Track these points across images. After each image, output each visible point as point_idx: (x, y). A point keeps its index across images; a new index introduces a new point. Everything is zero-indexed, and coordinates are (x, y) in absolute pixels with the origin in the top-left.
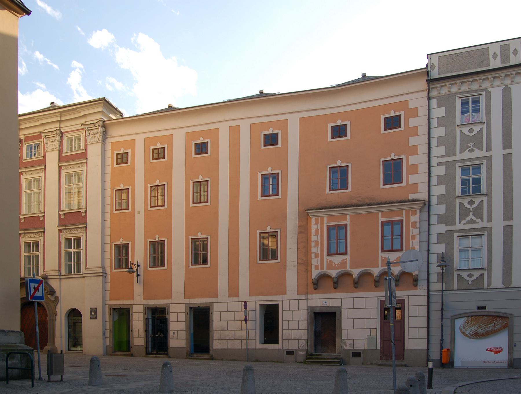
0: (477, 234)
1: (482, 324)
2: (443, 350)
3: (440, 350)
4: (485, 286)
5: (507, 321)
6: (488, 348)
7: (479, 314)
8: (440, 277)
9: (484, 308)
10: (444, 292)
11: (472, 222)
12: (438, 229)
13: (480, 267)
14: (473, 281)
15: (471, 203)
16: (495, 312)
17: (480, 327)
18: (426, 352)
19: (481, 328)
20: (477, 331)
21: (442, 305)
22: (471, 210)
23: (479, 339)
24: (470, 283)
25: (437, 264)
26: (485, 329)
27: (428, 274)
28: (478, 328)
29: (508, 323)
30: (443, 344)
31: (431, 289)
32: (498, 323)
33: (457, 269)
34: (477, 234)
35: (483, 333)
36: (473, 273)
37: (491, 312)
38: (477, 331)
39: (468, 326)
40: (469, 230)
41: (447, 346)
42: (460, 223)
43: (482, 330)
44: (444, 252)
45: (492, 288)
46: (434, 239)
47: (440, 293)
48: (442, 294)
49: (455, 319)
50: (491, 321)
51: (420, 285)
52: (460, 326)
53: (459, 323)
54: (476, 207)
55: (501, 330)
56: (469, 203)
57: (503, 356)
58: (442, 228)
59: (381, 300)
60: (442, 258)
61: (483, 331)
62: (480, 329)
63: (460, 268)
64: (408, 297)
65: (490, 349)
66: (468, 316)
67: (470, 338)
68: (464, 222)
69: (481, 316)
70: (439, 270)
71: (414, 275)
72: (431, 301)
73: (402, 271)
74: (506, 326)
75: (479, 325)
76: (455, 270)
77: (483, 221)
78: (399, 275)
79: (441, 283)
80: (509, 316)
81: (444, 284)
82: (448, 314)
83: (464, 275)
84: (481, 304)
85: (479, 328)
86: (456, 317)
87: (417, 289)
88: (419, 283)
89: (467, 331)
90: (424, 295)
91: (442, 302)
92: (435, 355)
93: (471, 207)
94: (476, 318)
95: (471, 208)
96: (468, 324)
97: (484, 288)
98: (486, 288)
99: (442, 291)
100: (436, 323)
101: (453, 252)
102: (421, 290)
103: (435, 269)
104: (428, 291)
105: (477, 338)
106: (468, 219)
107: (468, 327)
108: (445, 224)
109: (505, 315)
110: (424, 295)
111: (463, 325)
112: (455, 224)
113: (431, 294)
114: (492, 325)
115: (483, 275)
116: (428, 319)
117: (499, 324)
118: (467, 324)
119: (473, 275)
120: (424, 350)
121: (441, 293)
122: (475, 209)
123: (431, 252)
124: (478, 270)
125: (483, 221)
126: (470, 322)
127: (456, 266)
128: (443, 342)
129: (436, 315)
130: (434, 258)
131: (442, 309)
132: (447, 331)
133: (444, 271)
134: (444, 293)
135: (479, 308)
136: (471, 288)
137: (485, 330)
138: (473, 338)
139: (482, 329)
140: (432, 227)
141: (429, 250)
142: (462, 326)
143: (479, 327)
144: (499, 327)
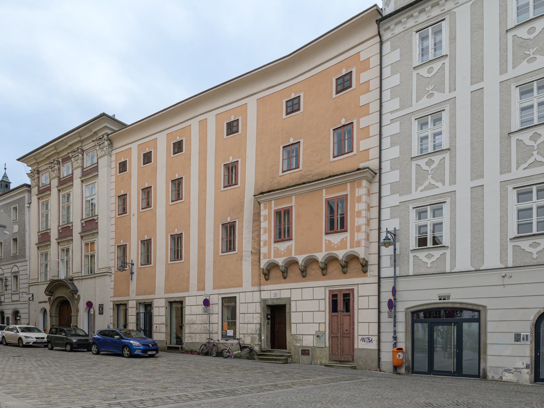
22: (430, 172)
31: (382, 275)
42: (416, 191)
45: (456, 271)
51: (370, 272)
64: (357, 285)
77: (444, 185)
87: (367, 276)
88: (370, 268)
95: (430, 170)
97: (447, 272)
102: (371, 277)
106: (426, 184)
121: (393, 280)
125: (444, 185)
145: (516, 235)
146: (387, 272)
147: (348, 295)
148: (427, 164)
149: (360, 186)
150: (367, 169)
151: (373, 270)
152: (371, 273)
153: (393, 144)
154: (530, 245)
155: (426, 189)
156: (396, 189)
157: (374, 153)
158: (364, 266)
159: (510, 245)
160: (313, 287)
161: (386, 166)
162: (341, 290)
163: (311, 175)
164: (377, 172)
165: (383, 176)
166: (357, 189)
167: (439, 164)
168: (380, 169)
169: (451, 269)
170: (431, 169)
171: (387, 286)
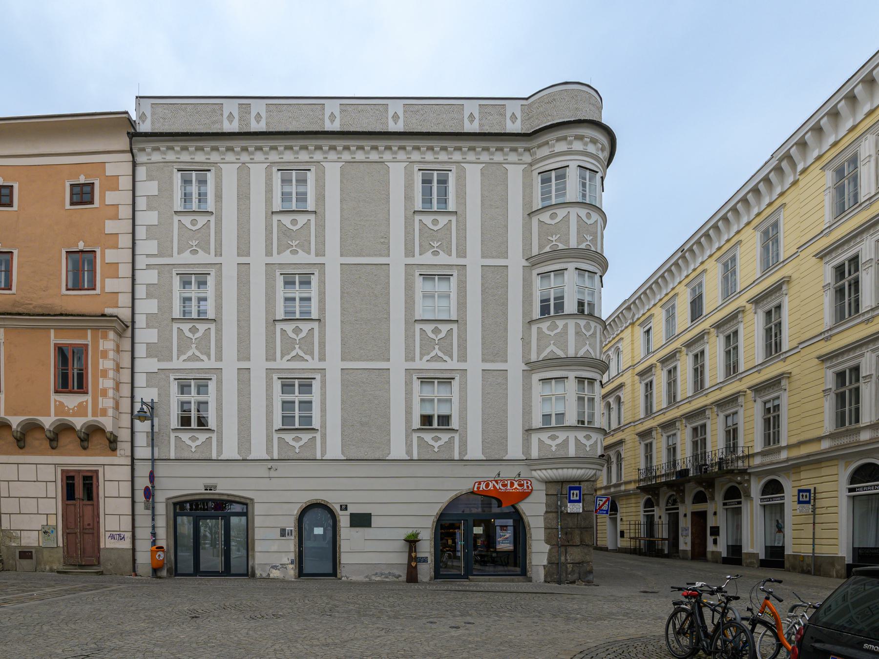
12: (146, 365)
15: (193, 330)
16: (228, 495)
22: (194, 340)
31: (137, 456)
37: (223, 494)
42: (178, 359)
77: (209, 359)
80: (248, 501)
87: (116, 456)
88: (119, 445)
95: (193, 338)
97: (213, 458)
102: (122, 457)
106: (190, 353)
108: (156, 359)
112: (171, 359)
125: (209, 359)
140: (137, 362)
146: (143, 452)
147: (91, 478)
149: (105, 337)
150: (116, 318)
151: (124, 447)
152: (122, 452)
153: (149, 296)
154: (293, 439)
155: (189, 359)
156: (153, 351)
157: (125, 300)
158: (112, 443)
159: (276, 436)
160: (36, 464)
161: (141, 321)
162: (79, 471)
163: (31, 304)
164: (129, 324)
165: (137, 331)
166: (101, 341)
167: (204, 334)
168: (133, 322)
169: (218, 456)
170: (195, 337)
171: (143, 470)
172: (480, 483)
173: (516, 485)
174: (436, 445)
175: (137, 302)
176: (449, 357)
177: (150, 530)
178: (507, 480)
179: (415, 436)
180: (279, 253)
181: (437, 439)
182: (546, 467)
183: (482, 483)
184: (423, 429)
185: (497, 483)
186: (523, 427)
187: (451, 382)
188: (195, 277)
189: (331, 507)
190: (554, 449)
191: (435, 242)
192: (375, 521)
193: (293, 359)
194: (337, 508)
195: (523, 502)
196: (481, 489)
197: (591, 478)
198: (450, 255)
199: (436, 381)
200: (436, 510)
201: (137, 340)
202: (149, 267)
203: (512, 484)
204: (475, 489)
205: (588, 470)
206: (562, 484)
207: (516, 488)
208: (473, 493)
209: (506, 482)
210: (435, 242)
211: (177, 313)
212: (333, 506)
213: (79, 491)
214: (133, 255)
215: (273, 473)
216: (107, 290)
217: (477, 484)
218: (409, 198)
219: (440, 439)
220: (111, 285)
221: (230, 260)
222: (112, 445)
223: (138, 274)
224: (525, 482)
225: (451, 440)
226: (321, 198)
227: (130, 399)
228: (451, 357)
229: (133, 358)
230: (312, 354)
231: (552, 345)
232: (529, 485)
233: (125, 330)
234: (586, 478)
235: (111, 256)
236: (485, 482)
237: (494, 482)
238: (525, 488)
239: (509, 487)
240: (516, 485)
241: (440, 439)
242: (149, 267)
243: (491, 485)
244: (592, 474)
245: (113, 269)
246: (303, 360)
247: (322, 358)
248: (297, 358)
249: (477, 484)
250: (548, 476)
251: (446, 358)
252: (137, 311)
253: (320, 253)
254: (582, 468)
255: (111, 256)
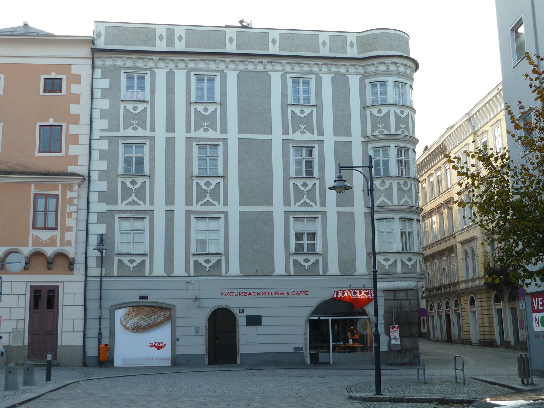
0: (139, 216)
1: (144, 316)
2: (101, 346)
3: (98, 346)
4: (147, 274)
5: (169, 313)
6: (150, 344)
7: (141, 304)
8: (100, 261)
9: (146, 297)
10: (103, 278)
11: (134, 203)
12: (98, 207)
13: (142, 253)
14: (134, 267)
15: (134, 183)
16: (157, 303)
17: (142, 319)
18: (82, 348)
19: (143, 320)
20: (139, 323)
21: (101, 293)
22: (133, 190)
23: (141, 332)
24: (131, 269)
25: (95, 247)
26: (147, 321)
27: (86, 257)
28: (140, 320)
29: (170, 315)
30: (101, 338)
31: (89, 274)
32: (160, 314)
33: (118, 253)
34: (139, 216)
35: (145, 326)
36: (134, 258)
37: (153, 302)
38: (139, 323)
39: (129, 317)
40: (131, 212)
41: (105, 341)
42: (122, 203)
43: (144, 323)
44: (104, 233)
46: (93, 218)
47: (99, 279)
48: (101, 281)
49: (115, 309)
50: (154, 313)
51: (76, 270)
52: (121, 318)
53: (120, 314)
54: (139, 188)
55: (164, 322)
56: (131, 183)
57: (166, 352)
58: (103, 207)
59: (31, 286)
60: (102, 240)
61: (145, 324)
62: (142, 322)
63: (120, 252)
64: (63, 282)
65: (153, 344)
66: (129, 307)
67: (131, 332)
68: (125, 202)
69: (143, 307)
70: (98, 253)
71: (70, 258)
72: (89, 287)
73: (54, 253)
74: (169, 318)
75: (141, 317)
76: (116, 254)
77: (145, 203)
78: (52, 257)
79: (100, 268)
80: (171, 307)
81: (104, 269)
82: (106, 304)
83: (125, 260)
84: (143, 293)
85: (141, 320)
86: (116, 307)
87: (73, 274)
88: (76, 266)
89: (128, 323)
90: (81, 281)
91: (101, 290)
92: (92, 352)
93: (133, 187)
94: (138, 309)
95: (133, 189)
96: (129, 316)
98: (148, 276)
99: (101, 277)
100: (93, 314)
101: (114, 234)
103: (93, 253)
104: (86, 276)
105: (138, 332)
106: (130, 199)
107: (129, 319)
108: (106, 203)
109: (167, 306)
110: (81, 281)
111: (124, 317)
112: (116, 204)
113: (89, 280)
114: (155, 317)
115: (144, 261)
116: (85, 309)
117: (162, 315)
118: (128, 315)
119: (135, 261)
120: (80, 346)
121: (100, 280)
122: (137, 190)
123: (90, 232)
124: (139, 256)
125: (145, 203)
126: (132, 313)
127: (116, 250)
128: (101, 336)
129: (93, 304)
130: (93, 240)
131: (101, 298)
132: (106, 323)
133: (104, 254)
134: (103, 280)
135: (141, 297)
136: (132, 275)
137: (147, 322)
138: (135, 332)
139: (144, 321)
140: (91, 205)
141: (87, 231)
142: (123, 318)
143: (141, 319)
144: (162, 319)
145: (195, 252)
147: (53, 291)
148: (131, 183)
151: (79, 268)
152: (78, 271)
153: (102, 158)
156: (103, 197)
157: (83, 160)
158: (71, 265)
159: (192, 259)
161: (95, 176)
164: (87, 178)
165: (92, 184)
167: (141, 186)
168: (89, 176)
169: (150, 273)
171: (94, 284)
172: (338, 292)
173: (363, 293)
174: (307, 265)
175: (92, 162)
176: (314, 203)
177: (97, 331)
178: (356, 290)
179: (292, 258)
180: (195, 130)
181: (307, 261)
182: (382, 281)
183: (340, 292)
184: (297, 254)
185: (350, 292)
186: (366, 252)
187: (316, 220)
188: (135, 145)
189: (232, 311)
190: (387, 268)
191: (303, 125)
192: (263, 320)
193: (205, 204)
194: (236, 311)
195: (367, 305)
196: (339, 296)
197: (413, 288)
198: (313, 134)
199: (305, 220)
200: (307, 312)
201: (92, 189)
202: (102, 138)
203: (360, 293)
204: (335, 296)
205: (411, 282)
206: (395, 292)
207: (363, 295)
208: (333, 299)
209: (356, 291)
210: (303, 125)
211: (121, 170)
212: (234, 310)
213: (43, 302)
214: (91, 129)
215: (190, 286)
216: (70, 153)
217: (336, 292)
218: (284, 95)
219: (309, 261)
220: (73, 150)
221: (160, 134)
222: (71, 267)
223: (93, 142)
224: (369, 290)
225: (317, 261)
226: (224, 94)
227: (85, 232)
228: (315, 202)
229: (88, 202)
230: (218, 200)
231: (383, 196)
232: (372, 293)
233: (83, 182)
234: (411, 287)
235: (73, 129)
236: (341, 291)
237: (348, 291)
238: (370, 295)
239: (358, 295)
240: (363, 293)
241: (309, 261)
242: (102, 138)
243: (346, 295)
244: (414, 286)
245: (74, 139)
246: (212, 204)
247: (226, 203)
248: (207, 203)
249: (336, 292)
250: (385, 287)
251: (312, 204)
252: (92, 169)
253: (224, 130)
254: (407, 281)
255: (73, 129)
